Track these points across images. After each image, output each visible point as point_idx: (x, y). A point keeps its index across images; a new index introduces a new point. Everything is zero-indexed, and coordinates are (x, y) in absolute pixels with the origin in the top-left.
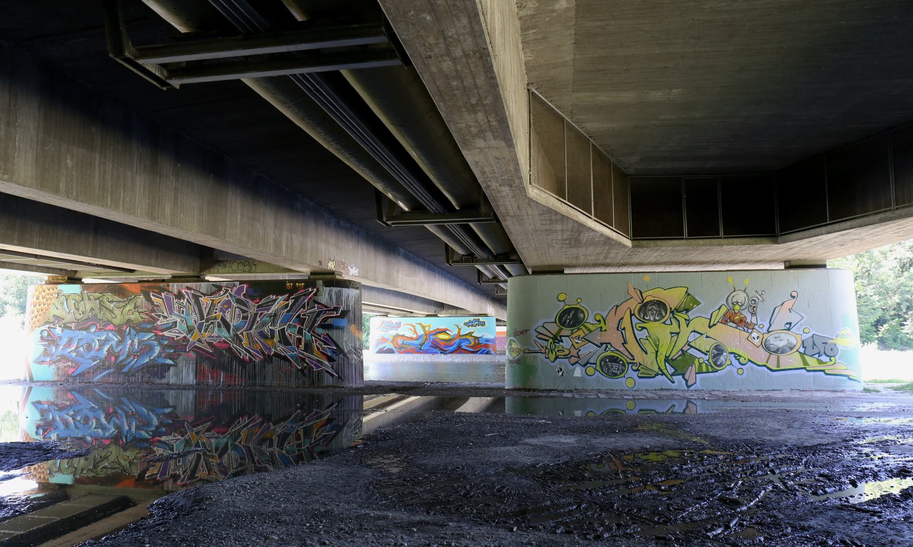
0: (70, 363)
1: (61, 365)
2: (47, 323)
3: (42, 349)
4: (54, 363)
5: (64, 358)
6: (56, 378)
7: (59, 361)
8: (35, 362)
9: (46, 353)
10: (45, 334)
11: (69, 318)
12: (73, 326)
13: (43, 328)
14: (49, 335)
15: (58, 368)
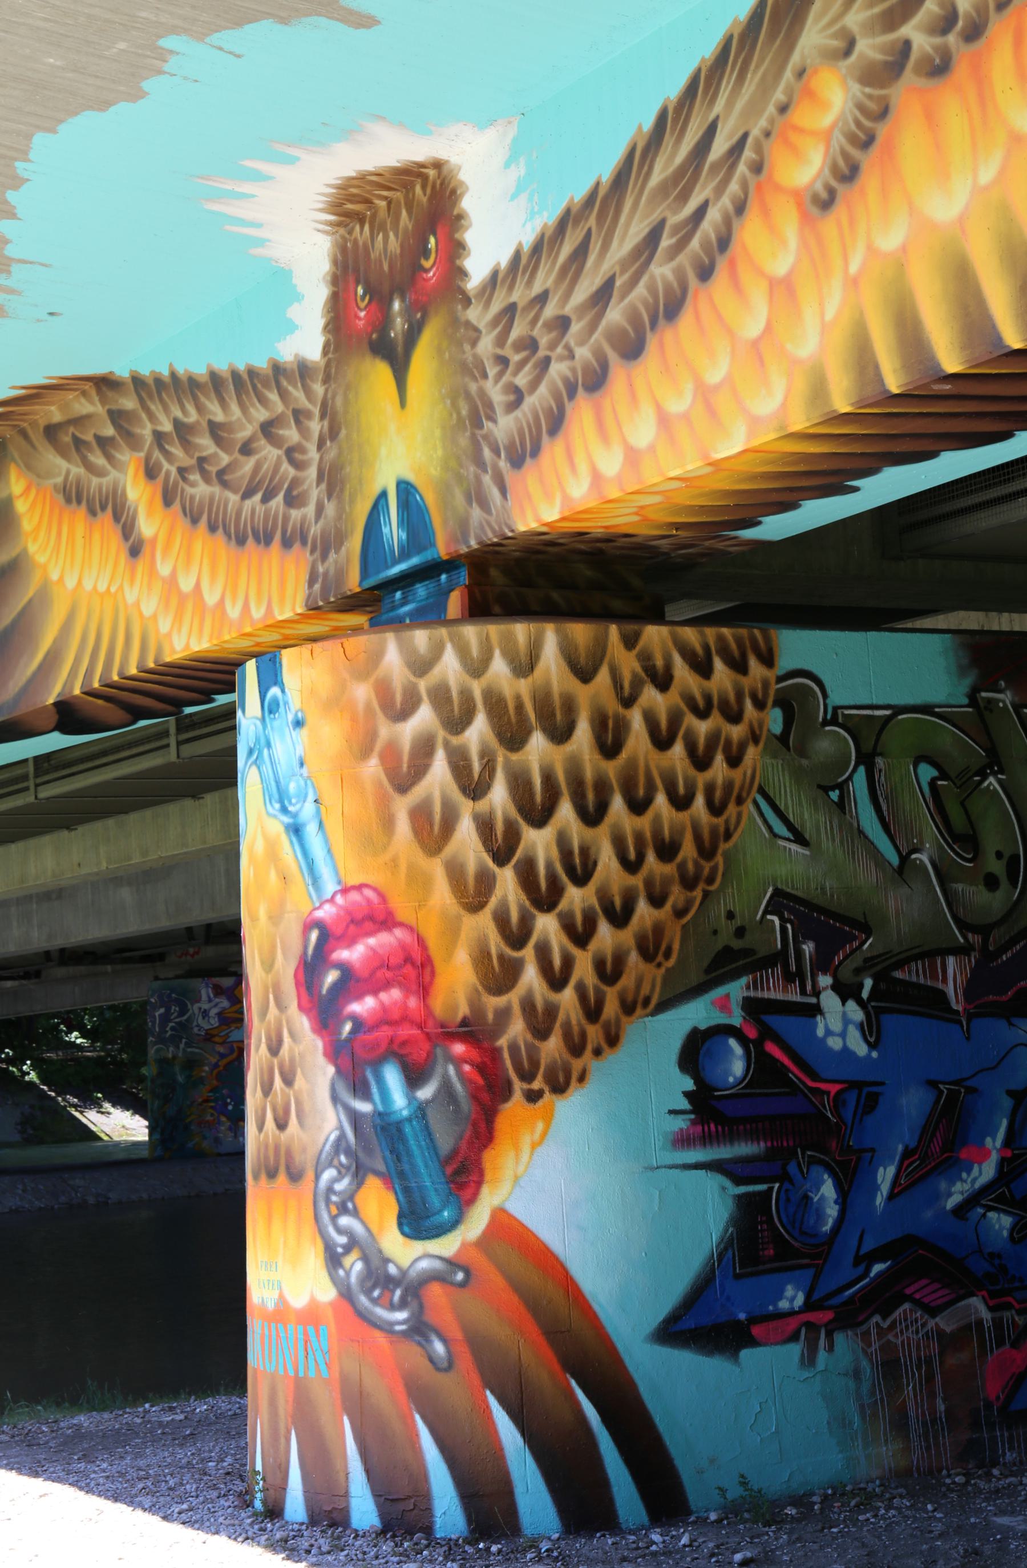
0: (978, 1306)
1: (909, 1326)
2: (722, 966)
3: (709, 1207)
4: (848, 1316)
5: (926, 1263)
6: (887, 1453)
7: (881, 1298)
8: (673, 1331)
9: (758, 1241)
10: (735, 1065)
11: (904, 911)
12: (953, 977)
13: (697, 1013)
14: (763, 1070)
15: (890, 1368)
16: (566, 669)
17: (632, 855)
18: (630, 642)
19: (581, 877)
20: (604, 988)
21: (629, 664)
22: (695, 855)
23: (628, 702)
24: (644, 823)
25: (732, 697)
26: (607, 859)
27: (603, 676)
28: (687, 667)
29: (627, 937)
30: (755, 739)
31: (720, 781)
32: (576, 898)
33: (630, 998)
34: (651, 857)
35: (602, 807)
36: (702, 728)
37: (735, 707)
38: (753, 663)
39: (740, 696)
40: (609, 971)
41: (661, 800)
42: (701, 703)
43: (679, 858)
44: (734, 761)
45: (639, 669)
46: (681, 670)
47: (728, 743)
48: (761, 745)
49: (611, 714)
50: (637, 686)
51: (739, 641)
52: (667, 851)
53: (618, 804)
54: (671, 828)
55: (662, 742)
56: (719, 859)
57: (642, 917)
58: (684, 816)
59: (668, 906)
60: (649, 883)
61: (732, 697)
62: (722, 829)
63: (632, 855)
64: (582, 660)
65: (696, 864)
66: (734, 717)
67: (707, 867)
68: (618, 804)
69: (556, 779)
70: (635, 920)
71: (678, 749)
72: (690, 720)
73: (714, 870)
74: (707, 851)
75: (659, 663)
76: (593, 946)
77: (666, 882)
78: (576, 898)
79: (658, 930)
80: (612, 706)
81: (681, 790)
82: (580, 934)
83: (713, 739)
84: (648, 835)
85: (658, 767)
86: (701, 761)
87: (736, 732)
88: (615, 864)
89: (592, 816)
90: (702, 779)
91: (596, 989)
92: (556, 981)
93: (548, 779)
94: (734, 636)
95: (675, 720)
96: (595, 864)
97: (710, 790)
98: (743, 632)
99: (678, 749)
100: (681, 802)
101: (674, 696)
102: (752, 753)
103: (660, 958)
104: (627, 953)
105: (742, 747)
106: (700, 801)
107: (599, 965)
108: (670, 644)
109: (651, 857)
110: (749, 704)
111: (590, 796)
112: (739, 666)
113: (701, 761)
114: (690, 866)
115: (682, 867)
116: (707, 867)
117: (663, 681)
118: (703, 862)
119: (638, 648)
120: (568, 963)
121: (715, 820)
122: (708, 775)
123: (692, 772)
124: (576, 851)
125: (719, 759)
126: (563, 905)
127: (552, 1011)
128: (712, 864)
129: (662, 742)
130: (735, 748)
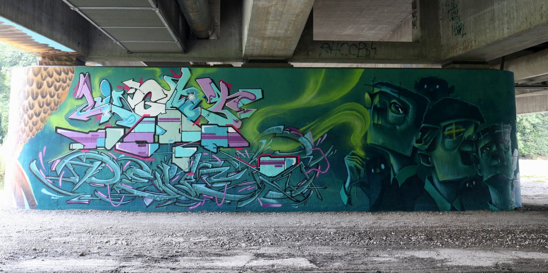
18: (45, 69)
19: (31, 109)
21: (45, 73)
23: (44, 80)
24: (45, 100)
26: (37, 106)
27: (39, 76)
29: (39, 118)
30: (69, 86)
32: (31, 112)
34: (45, 106)
35: (37, 97)
38: (70, 73)
39: (66, 79)
40: (35, 124)
41: (48, 96)
44: (63, 90)
46: (55, 75)
50: (46, 77)
51: (67, 70)
52: (48, 105)
53: (40, 97)
55: (49, 86)
58: (52, 99)
60: (44, 110)
66: (65, 82)
67: (56, 108)
68: (40, 97)
71: (53, 88)
72: (56, 83)
74: (56, 105)
75: (51, 73)
76: (32, 120)
77: (48, 110)
78: (31, 112)
79: (45, 118)
80: (40, 80)
82: (31, 118)
83: (60, 86)
87: (65, 85)
89: (35, 98)
90: (57, 93)
92: (26, 125)
93: (28, 92)
95: (53, 83)
97: (58, 95)
99: (53, 88)
100: (52, 96)
101: (53, 79)
102: (68, 88)
105: (66, 87)
106: (56, 96)
107: (33, 123)
109: (45, 106)
110: (68, 80)
111: (35, 95)
112: (67, 74)
113: (57, 90)
116: (56, 108)
117: (51, 76)
120: (28, 123)
122: (58, 92)
123: (55, 91)
125: (61, 89)
126: (28, 113)
127: (25, 130)
129: (49, 86)
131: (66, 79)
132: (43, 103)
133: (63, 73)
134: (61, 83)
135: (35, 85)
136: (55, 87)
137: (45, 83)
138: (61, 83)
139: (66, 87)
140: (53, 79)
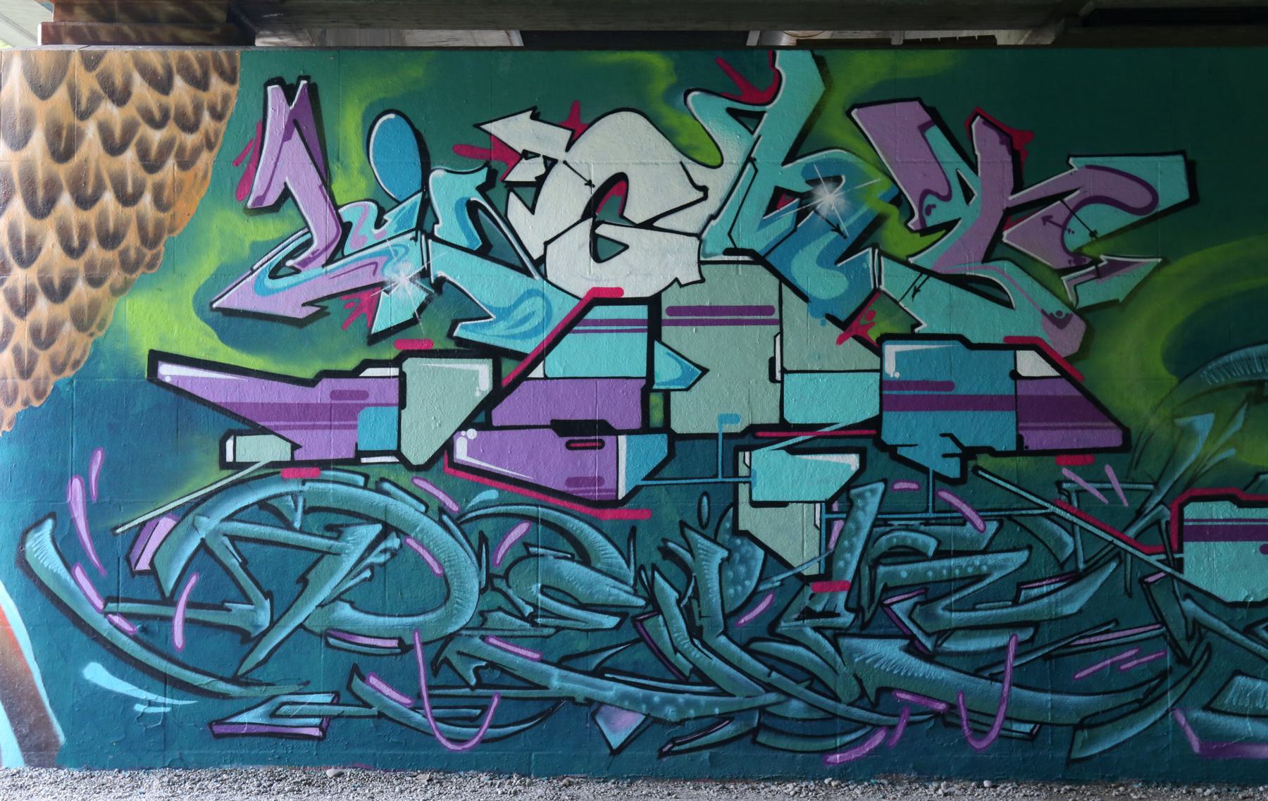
16: (26, 84)
17: (76, 243)
18: (91, 63)
19: (25, 262)
20: (38, 351)
21: (87, 83)
22: (138, 244)
23: (84, 116)
24: (91, 216)
25: (190, 110)
27: (61, 94)
28: (146, 85)
29: (63, 310)
30: (210, 145)
31: (169, 181)
32: (20, 277)
33: (60, 360)
34: (94, 245)
35: (51, 202)
36: (157, 137)
37: (192, 118)
39: (198, 109)
40: (44, 337)
41: (108, 198)
42: (157, 115)
43: (122, 246)
44: (184, 165)
45: (97, 87)
46: (140, 87)
47: (181, 150)
48: (216, 150)
49: (65, 125)
50: (94, 101)
51: (202, 62)
52: (110, 239)
53: (65, 201)
54: (116, 220)
55: (114, 147)
56: (161, 247)
57: (79, 295)
58: (131, 212)
59: (106, 286)
60: (90, 266)
61: (190, 110)
62: (167, 223)
63: (76, 243)
64: (42, 81)
65: (138, 251)
67: (149, 254)
68: (65, 201)
69: (11, 179)
70: (72, 297)
71: (130, 155)
72: (145, 130)
73: (155, 258)
74: (150, 239)
75: (118, 80)
76: (30, 317)
77: (107, 267)
79: (94, 306)
81: (130, 189)
83: (166, 148)
84: (93, 226)
85: (108, 171)
86: (151, 164)
87: (191, 140)
88: (58, 251)
89: (41, 209)
90: (151, 180)
91: (31, 353)
94: (197, 57)
95: (129, 129)
96: (40, 249)
98: (207, 52)
99: (130, 155)
100: (127, 199)
101: (130, 110)
102: (206, 157)
103: (93, 328)
104: (61, 324)
105: (196, 152)
106: (147, 199)
107: (35, 333)
108: (131, 65)
109: (94, 245)
110: (206, 116)
111: (40, 193)
114: (132, 254)
115: (124, 254)
116: (149, 254)
117: (121, 97)
118: (145, 250)
119: (98, 70)
121: (162, 215)
122: (158, 177)
123: (142, 173)
124: (24, 238)
125: (171, 163)
128: (154, 251)
129: (114, 147)
130: (188, 153)
131: (198, 109)
132: (84, 229)
133: (179, 82)
134: (171, 130)
135: (38, 142)
136: (143, 154)
137: (91, 130)
138: (171, 130)
139: (196, 152)
140: (130, 110)
